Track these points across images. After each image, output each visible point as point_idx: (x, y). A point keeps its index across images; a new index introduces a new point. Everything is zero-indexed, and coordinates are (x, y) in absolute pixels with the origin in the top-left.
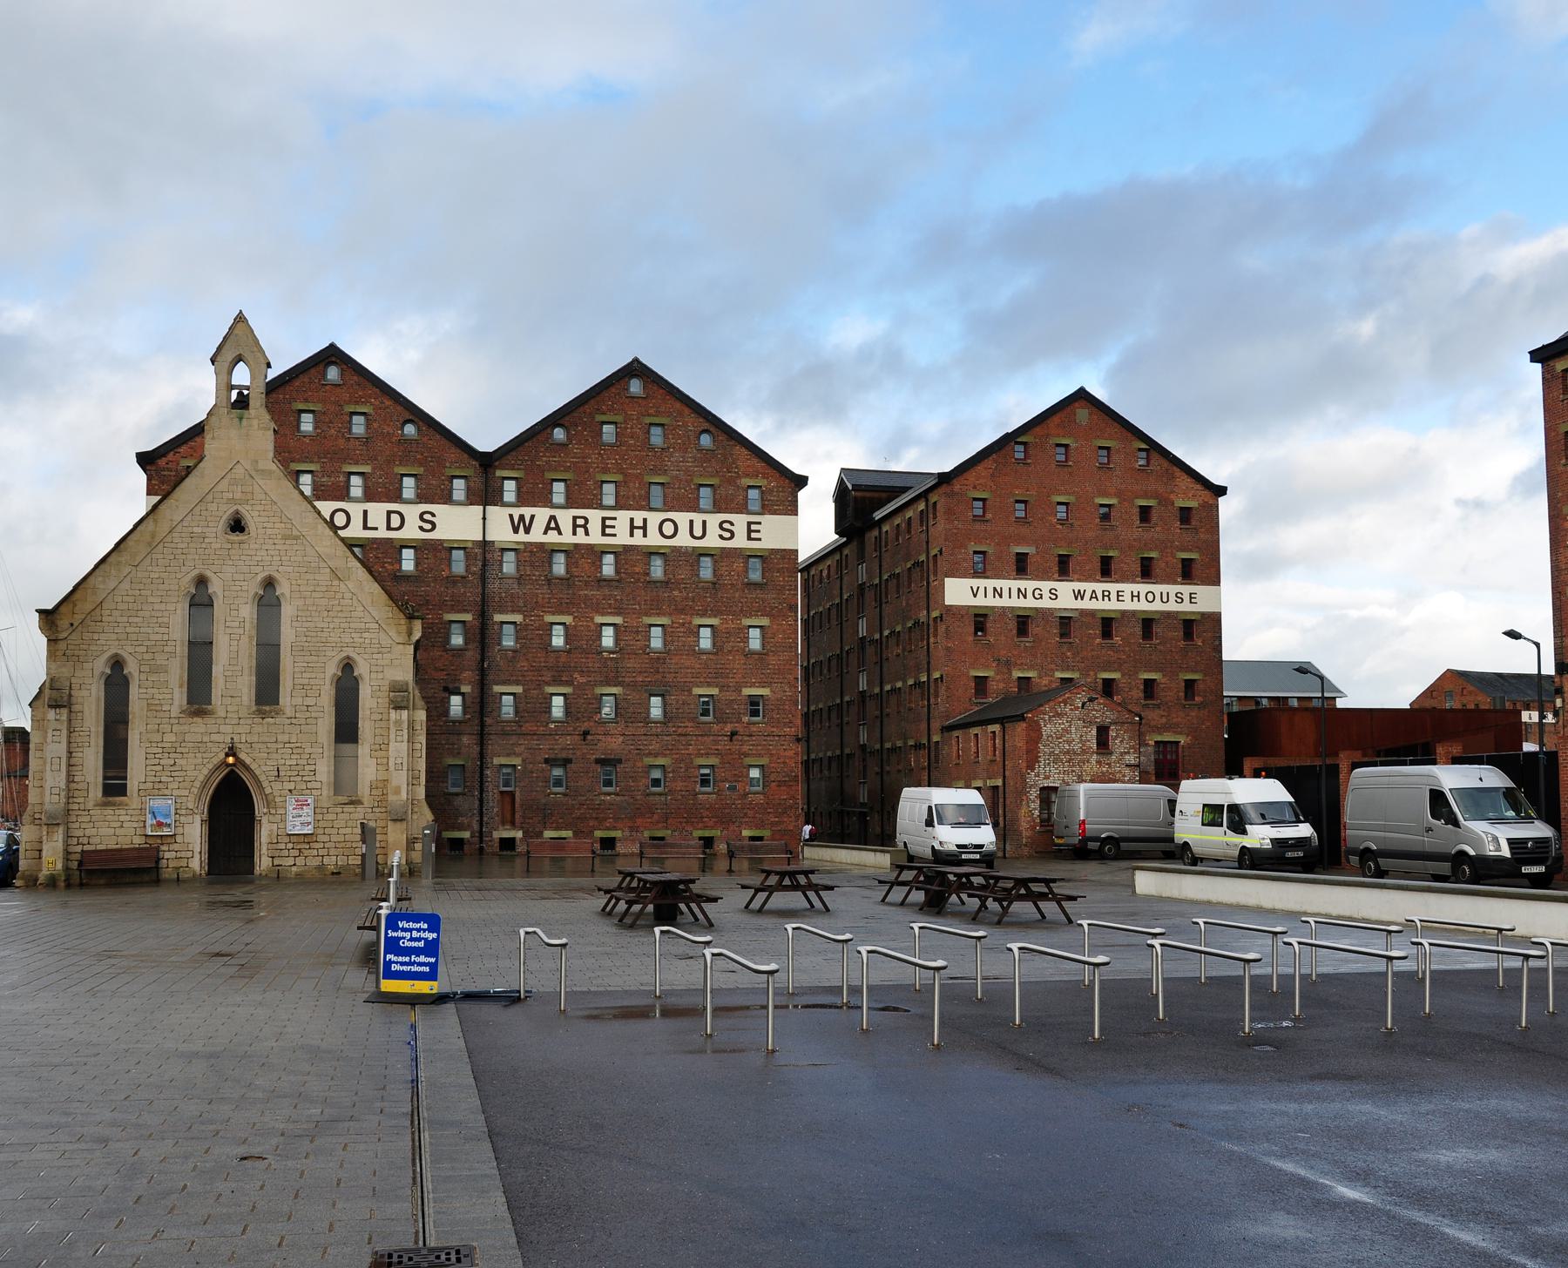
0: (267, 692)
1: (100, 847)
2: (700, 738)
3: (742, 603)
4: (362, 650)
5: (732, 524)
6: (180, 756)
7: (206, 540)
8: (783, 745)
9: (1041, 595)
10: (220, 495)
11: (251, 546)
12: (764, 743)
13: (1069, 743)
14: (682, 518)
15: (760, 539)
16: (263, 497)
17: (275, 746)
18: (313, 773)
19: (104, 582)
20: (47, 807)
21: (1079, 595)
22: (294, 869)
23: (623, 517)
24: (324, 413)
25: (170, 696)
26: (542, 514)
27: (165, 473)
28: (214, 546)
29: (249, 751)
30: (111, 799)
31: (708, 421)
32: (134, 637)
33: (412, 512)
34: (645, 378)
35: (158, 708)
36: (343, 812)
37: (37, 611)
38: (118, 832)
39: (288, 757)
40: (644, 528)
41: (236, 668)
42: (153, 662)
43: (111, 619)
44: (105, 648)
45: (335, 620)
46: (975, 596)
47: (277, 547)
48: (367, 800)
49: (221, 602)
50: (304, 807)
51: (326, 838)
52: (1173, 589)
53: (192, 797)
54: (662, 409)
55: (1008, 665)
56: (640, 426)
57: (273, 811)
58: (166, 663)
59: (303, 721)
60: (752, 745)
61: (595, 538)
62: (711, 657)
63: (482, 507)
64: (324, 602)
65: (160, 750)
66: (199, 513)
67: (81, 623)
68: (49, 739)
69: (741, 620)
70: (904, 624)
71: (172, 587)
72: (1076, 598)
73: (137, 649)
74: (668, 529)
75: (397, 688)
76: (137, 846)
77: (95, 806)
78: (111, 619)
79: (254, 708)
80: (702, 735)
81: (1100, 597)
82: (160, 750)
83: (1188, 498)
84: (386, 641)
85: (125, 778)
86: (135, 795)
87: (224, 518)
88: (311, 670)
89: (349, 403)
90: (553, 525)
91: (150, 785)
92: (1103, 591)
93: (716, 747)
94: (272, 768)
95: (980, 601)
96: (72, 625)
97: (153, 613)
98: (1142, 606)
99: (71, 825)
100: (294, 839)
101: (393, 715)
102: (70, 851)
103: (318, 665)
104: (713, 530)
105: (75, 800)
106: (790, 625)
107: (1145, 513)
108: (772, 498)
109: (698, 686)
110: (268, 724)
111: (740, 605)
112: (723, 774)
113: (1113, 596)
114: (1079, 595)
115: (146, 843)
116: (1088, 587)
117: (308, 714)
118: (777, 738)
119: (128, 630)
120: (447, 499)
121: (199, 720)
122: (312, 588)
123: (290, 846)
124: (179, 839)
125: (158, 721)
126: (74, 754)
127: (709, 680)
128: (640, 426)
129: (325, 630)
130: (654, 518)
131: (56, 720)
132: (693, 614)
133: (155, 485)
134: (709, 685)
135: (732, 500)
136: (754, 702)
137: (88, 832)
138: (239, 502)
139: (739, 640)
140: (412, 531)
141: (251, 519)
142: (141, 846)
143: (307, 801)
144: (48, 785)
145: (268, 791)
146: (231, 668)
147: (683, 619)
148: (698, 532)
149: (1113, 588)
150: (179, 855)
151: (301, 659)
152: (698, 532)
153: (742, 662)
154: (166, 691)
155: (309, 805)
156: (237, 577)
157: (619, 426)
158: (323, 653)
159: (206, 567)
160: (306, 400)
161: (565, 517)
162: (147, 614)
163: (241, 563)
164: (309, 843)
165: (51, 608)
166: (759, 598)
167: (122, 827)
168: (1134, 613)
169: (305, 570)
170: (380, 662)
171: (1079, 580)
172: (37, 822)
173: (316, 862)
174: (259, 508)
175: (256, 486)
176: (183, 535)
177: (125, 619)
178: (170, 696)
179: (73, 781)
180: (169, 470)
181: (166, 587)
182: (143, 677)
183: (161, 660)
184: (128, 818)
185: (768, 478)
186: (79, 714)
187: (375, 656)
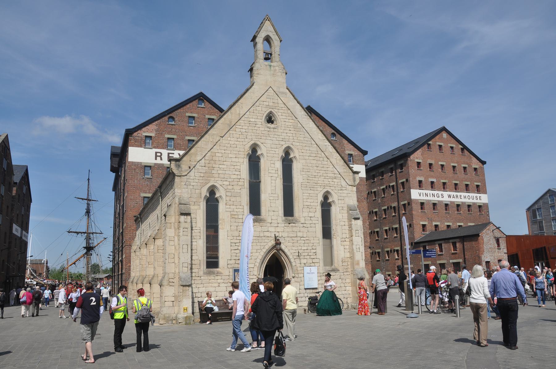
9: (439, 196)
13: (491, 244)
16: (283, 106)
21: (449, 196)
24: (198, 118)
25: (242, 210)
27: (137, 138)
30: (212, 270)
32: (222, 176)
35: (236, 217)
39: (303, 245)
41: (274, 195)
42: (233, 191)
46: (420, 196)
48: (341, 269)
53: (256, 269)
55: (431, 221)
58: (239, 191)
59: (309, 225)
64: (315, 162)
66: (253, 111)
67: (194, 167)
68: (181, 234)
70: (380, 209)
71: (241, 150)
72: (449, 198)
73: (225, 183)
75: (350, 209)
79: (284, 218)
81: (455, 197)
85: (217, 257)
89: (208, 114)
92: (456, 195)
94: (295, 251)
96: (190, 168)
97: (232, 163)
101: (354, 222)
108: (356, 159)
113: (459, 197)
114: (449, 196)
117: (311, 222)
119: (219, 172)
125: (237, 224)
133: (133, 142)
138: (272, 107)
141: (280, 116)
145: (294, 264)
146: (273, 195)
149: (459, 194)
151: (306, 192)
154: (241, 207)
159: (258, 140)
160: (191, 113)
162: (229, 163)
167: (219, 286)
168: (465, 203)
169: (305, 145)
171: (449, 191)
176: (245, 122)
177: (217, 166)
180: (139, 137)
181: (238, 149)
182: (228, 198)
184: (222, 281)
185: (354, 151)
187: (340, 191)
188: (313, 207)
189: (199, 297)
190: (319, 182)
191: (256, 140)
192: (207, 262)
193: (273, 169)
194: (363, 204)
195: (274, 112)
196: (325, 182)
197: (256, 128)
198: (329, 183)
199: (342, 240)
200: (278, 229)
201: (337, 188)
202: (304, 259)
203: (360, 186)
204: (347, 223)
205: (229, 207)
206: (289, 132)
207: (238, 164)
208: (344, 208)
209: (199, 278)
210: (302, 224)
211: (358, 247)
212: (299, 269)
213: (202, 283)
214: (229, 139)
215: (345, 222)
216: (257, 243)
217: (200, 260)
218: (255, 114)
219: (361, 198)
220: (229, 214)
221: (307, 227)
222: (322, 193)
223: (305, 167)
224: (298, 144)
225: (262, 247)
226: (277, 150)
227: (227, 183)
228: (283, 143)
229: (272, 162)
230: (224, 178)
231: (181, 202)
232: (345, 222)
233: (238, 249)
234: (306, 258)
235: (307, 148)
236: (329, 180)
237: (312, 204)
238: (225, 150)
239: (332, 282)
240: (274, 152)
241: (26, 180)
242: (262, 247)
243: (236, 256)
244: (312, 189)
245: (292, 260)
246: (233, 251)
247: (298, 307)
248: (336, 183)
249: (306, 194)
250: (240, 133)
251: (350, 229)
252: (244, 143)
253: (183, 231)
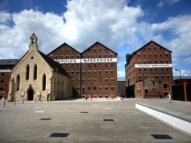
0: (35, 78)
14: (103, 59)
21: (152, 66)
23: (96, 59)
26: (87, 59)
33: (73, 60)
40: (99, 60)
52: (165, 64)
55: (144, 75)
61: (93, 62)
63: (80, 59)
74: (101, 60)
83: (166, 53)
84: (49, 71)
90: (88, 61)
95: (140, 67)
98: (161, 67)
107: (161, 55)
114: (152, 66)
116: (154, 65)
120: (77, 58)
130: (100, 59)
140: (73, 62)
148: (105, 60)
149: (157, 65)
152: (105, 60)
161: (90, 60)
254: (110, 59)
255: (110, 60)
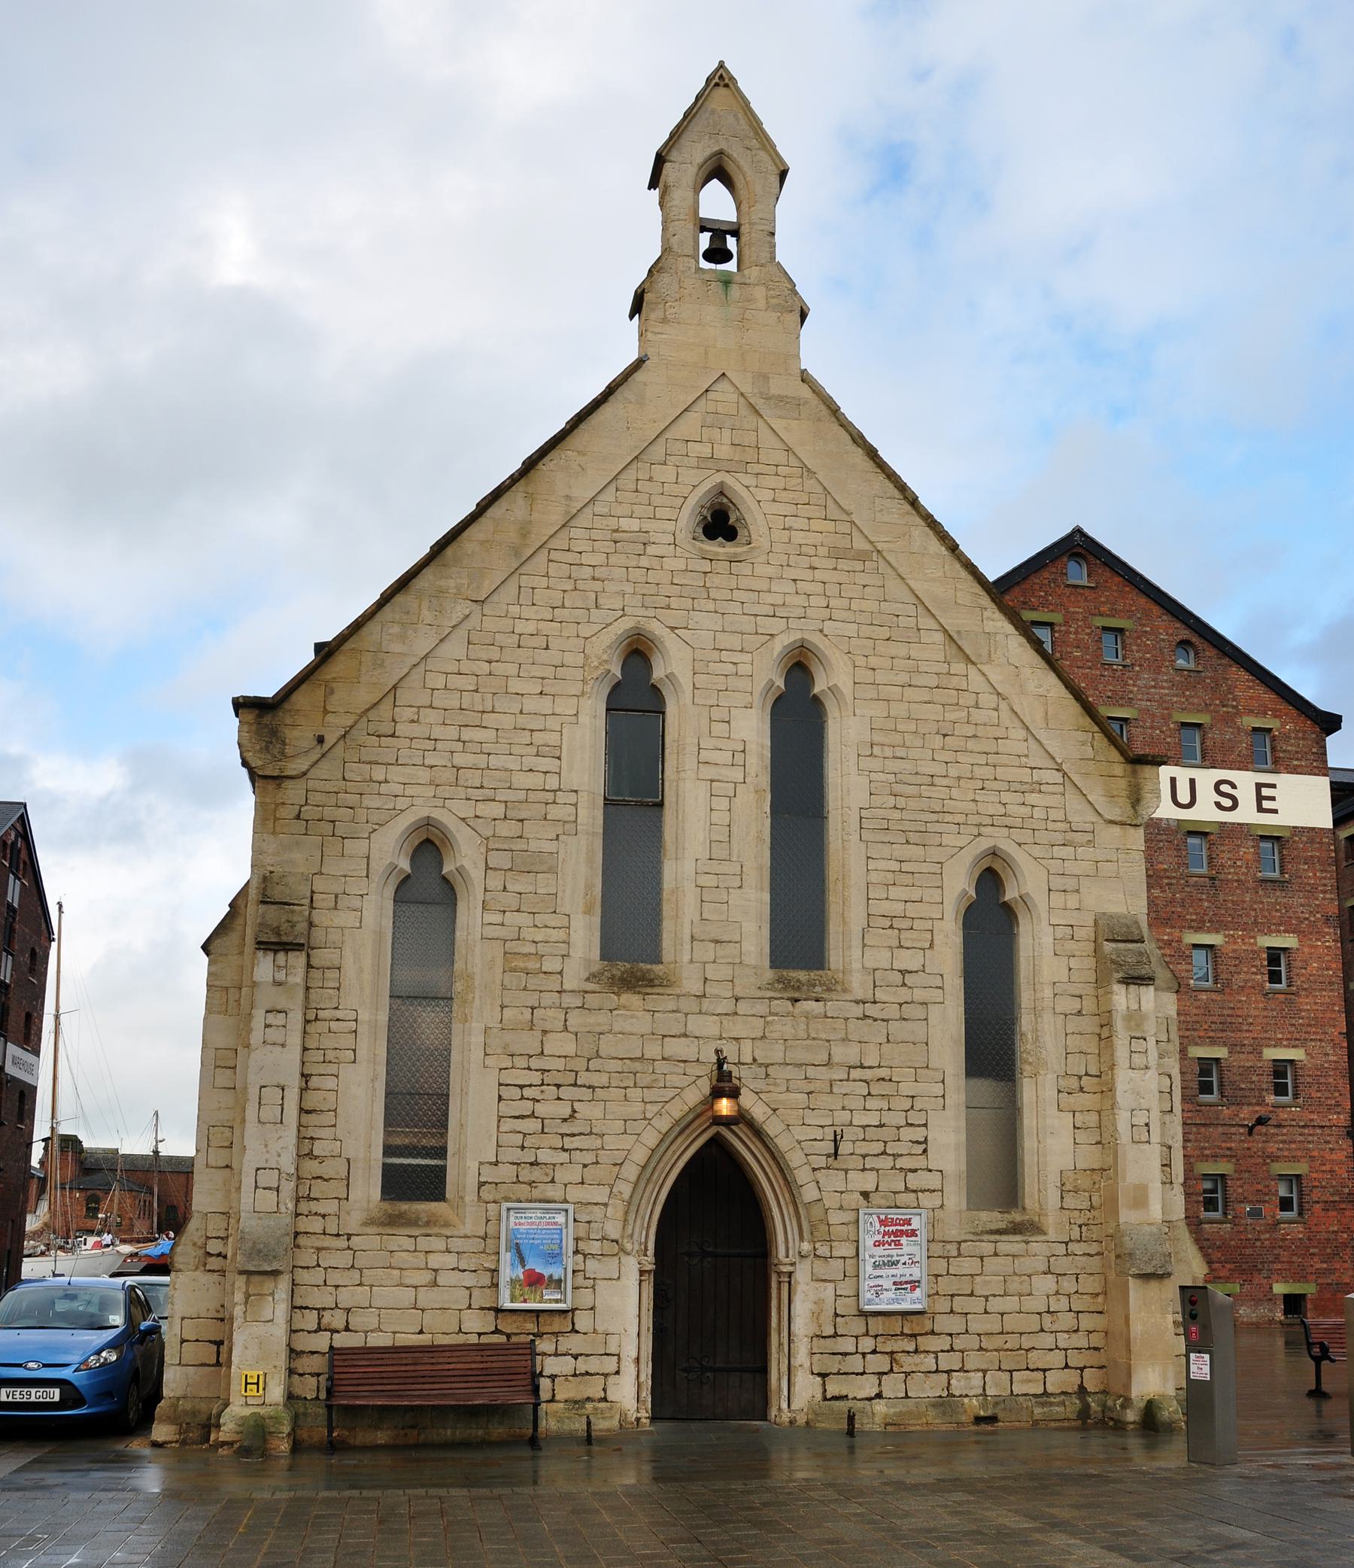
1: (377, 1340)
2: (1203, 1130)
3: (1255, 910)
4: (1025, 836)
5: (1234, 786)
6: (586, 1094)
7: (651, 550)
8: (1328, 1142)
10: (678, 448)
11: (759, 570)
12: (1301, 1138)
15: (1275, 811)
16: (781, 457)
17: (824, 1074)
18: (919, 1149)
19: (402, 638)
20: (248, 1223)
22: (880, 1407)
25: (561, 935)
28: (670, 564)
29: (760, 1085)
30: (404, 1206)
31: (1188, 626)
32: (475, 779)
34: (1091, 558)
35: (532, 965)
36: (996, 1254)
37: (241, 705)
38: (426, 1297)
39: (858, 1103)
41: (725, 868)
42: (520, 845)
43: (416, 730)
44: (401, 803)
45: (961, 757)
47: (819, 575)
48: (1053, 1223)
49: (689, 701)
50: (904, 1240)
51: (955, 1324)
53: (616, 1210)
54: (1120, 607)
56: (1088, 631)
57: (823, 1250)
59: (893, 1012)
60: (1282, 1142)
62: (1214, 996)
64: (931, 712)
65: (536, 1078)
68: (256, 1037)
69: (1254, 937)
71: (569, 659)
73: (484, 809)
76: (474, 1339)
77: (370, 1222)
78: (416, 730)
79: (769, 975)
80: (1205, 1125)
82: (536, 1078)
84: (1081, 816)
85: (441, 1152)
86: (470, 1196)
87: (693, 501)
88: (907, 879)
91: (507, 1172)
93: (1228, 1145)
96: (321, 740)
97: (522, 720)
99: (303, 1276)
100: (877, 1325)
101: (1121, 998)
102: (299, 1348)
103: (925, 868)
104: (1206, 795)
105: (314, 1206)
106: (1327, 947)
109: (1196, 1044)
110: (807, 1016)
111: (1253, 913)
112: (1240, 1190)
115: (497, 1331)
117: (904, 994)
118: (1318, 1131)
119: (459, 760)
121: (630, 999)
122: (904, 678)
123: (867, 1344)
124: (583, 1321)
126: (314, 1082)
127: (1211, 1034)
128: (1088, 631)
129: (927, 780)
131: (278, 984)
132: (1184, 927)
134: (1213, 1042)
135: (1232, 749)
136: (1280, 1069)
137: (345, 1298)
139: (1254, 970)
142: (484, 1339)
143: (908, 1222)
144: (251, 1160)
145: (809, 1194)
146: (715, 867)
147: (1169, 934)
148: (1184, 797)
150: (582, 1365)
151: (886, 850)
152: (1184, 797)
153: (1261, 1005)
155: (913, 1233)
156: (725, 641)
157: (1057, 628)
158: (937, 840)
159: (651, 613)
162: (507, 721)
163: (735, 607)
164: (914, 1336)
165: (271, 696)
166: (1279, 904)
169: (885, 632)
170: (1070, 867)
172: (214, 1263)
173: (930, 1389)
174: (771, 481)
175: (764, 432)
177: (452, 732)
178: (561, 935)
179: (310, 1155)
182: (495, 881)
183: (539, 837)
184: (451, 1260)
185: (1280, 717)
186: (329, 974)
187: (1058, 851)
188: (917, 924)
189: (338, 1332)
190: (950, 805)
191: (641, 612)
192: (388, 1171)
193: (720, 744)
194: (1320, 943)
195: (738, 487)
196: (982, 808)
197: (644, 562)
198: (1002, 811)
199: (1063, 1083)
200: (737, 1028)
201: (1042, 837)
202: (864, 1170)
203: (1306, 867)
204: (1089, 1005)
205: (497, 918)
206: (808, 575)
207: (553, 723)
208: (1080, 933)
209: (342, 1243)
210: (857, 1002)
211: (1141, 1119)
212: (835, 1218)
213: (353, 1266)
214: (514, 610)
215: (1080, 997)
216: (625, 1088)
217: (348, 1160)
218: (644, 498)
219: (1312, 919)
220: (497, 949)
221: (883, 1020)
222: (968, 857)
223: (878, 738)
224: (851, 629)
225: (652, 1109)
226: (747, 657)
227: (498, 810)
228: (775, 625)
229: (716, 713)
230: (482, 787)
231: (268, 893)
232: (1080, 997)
233: (533, 1115)
234: (872, 1169)
235: (900, 650)
236: (1006, 797)
237: (912, 910)
238: (490, 662)
239: (605, 1294)
240: (730, 669)
241: (24, 855)
242: (652, 1109)
243: (523, 1147)
244: (914, 837)
245: (802, 1176)
246: (508, 1125)
247: (825, 1399)
248: (1039, 813)
249: (882, 865)
250: (569, 586)
251: (1105, 1033)
252: (586, 631)
253: (267, 1026)
254: (1245, 781)
255: (1246, 794)
